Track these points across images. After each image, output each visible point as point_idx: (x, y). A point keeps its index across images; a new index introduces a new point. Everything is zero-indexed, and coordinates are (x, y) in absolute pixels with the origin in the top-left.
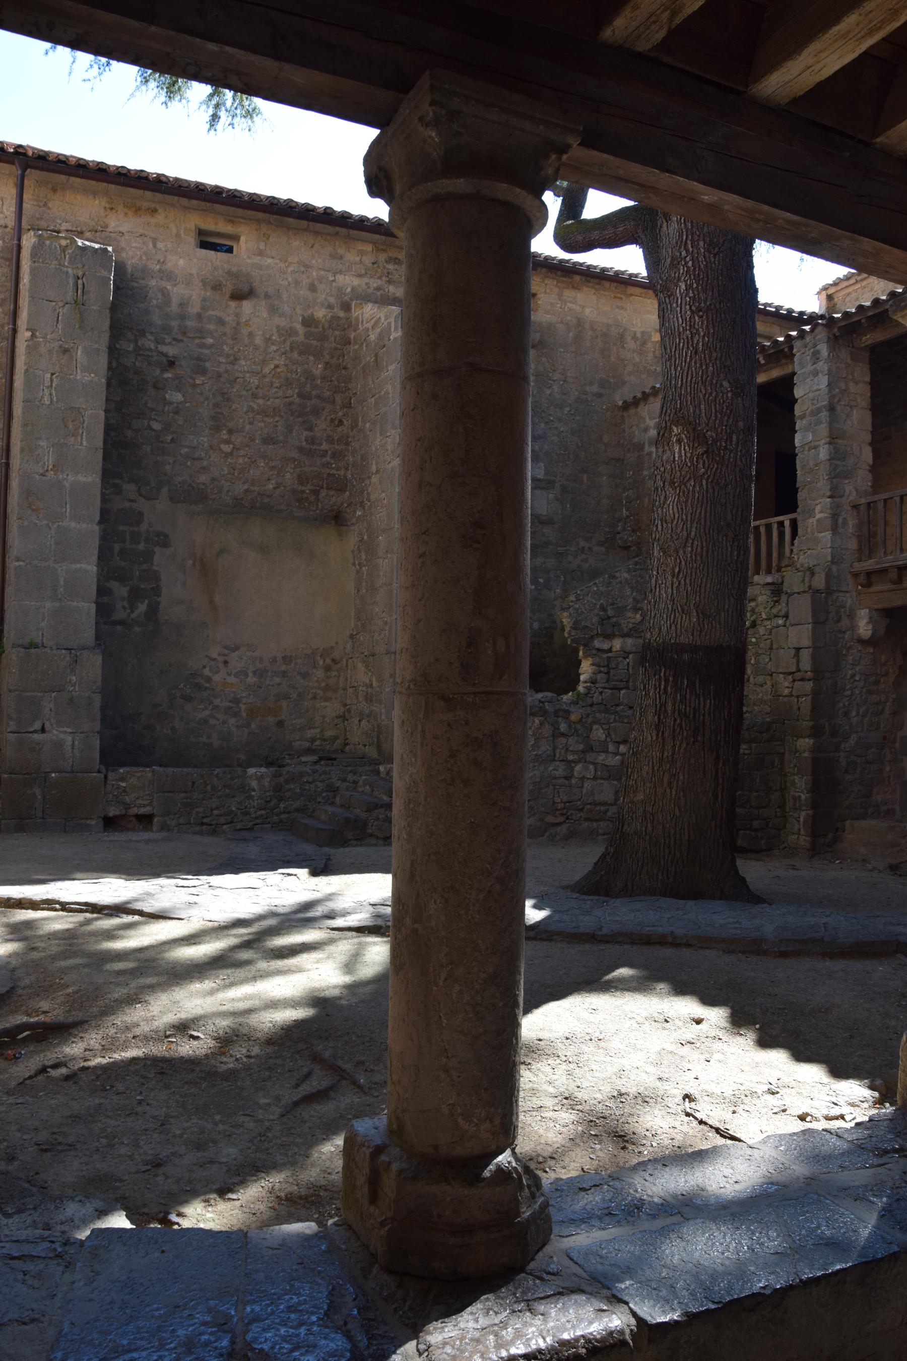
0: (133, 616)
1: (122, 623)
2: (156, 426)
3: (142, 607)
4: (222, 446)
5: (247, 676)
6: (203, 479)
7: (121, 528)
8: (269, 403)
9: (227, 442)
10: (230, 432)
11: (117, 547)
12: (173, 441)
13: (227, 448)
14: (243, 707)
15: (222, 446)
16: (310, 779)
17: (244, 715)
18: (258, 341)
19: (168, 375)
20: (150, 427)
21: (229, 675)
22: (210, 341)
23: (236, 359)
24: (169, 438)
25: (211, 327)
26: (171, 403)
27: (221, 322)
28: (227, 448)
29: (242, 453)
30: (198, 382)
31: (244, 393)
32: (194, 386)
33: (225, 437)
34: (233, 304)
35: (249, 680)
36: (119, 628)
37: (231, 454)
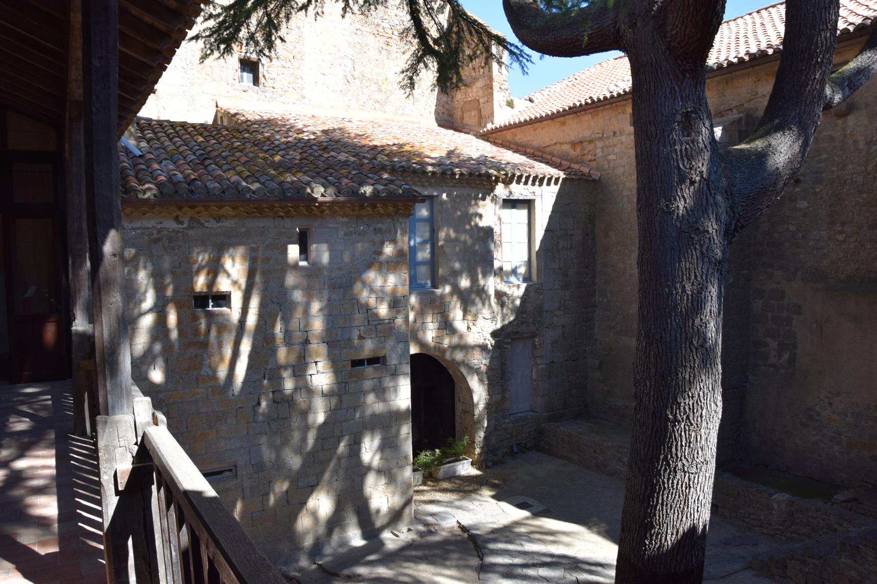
0: (781, 361)
1: (773, 366)
2: (792, 228)
3: (786, 356)
4: (837, 236)
5: (847, 416)
6: (825, 262)
7: (772, 302)
8: (872, 195)
9: (841, 232)
10: (843, 224)
11: (770, 315)
12: (803, 237)
13: (840, 237)
14: (844, 439)
15: (837, 236)
16: (814, 515)
17: (845, 445)
18: (861, 145)
19: (798, 189)
20: (788, 229)
21: (834, 413)
22: (825, 156)
23: (845, 165)
24: (800, 235)
25: (825, 145)
26: (801, 210)
27: (832, 139)
28: (840, 237)
29: (853, 239)
30: (817, 190)
31: (852, 191)
32: (816, 193)
33: (839, 229)
34: (840, 122)
35: (848, 419)
36: (771, 369)
37: (844, 241)
